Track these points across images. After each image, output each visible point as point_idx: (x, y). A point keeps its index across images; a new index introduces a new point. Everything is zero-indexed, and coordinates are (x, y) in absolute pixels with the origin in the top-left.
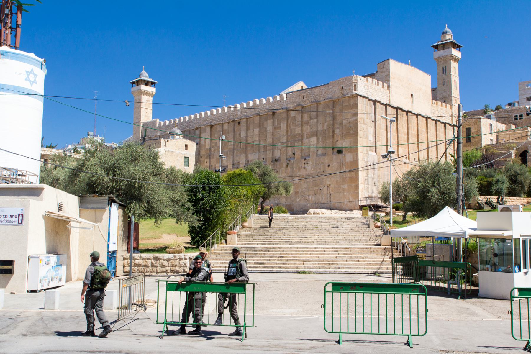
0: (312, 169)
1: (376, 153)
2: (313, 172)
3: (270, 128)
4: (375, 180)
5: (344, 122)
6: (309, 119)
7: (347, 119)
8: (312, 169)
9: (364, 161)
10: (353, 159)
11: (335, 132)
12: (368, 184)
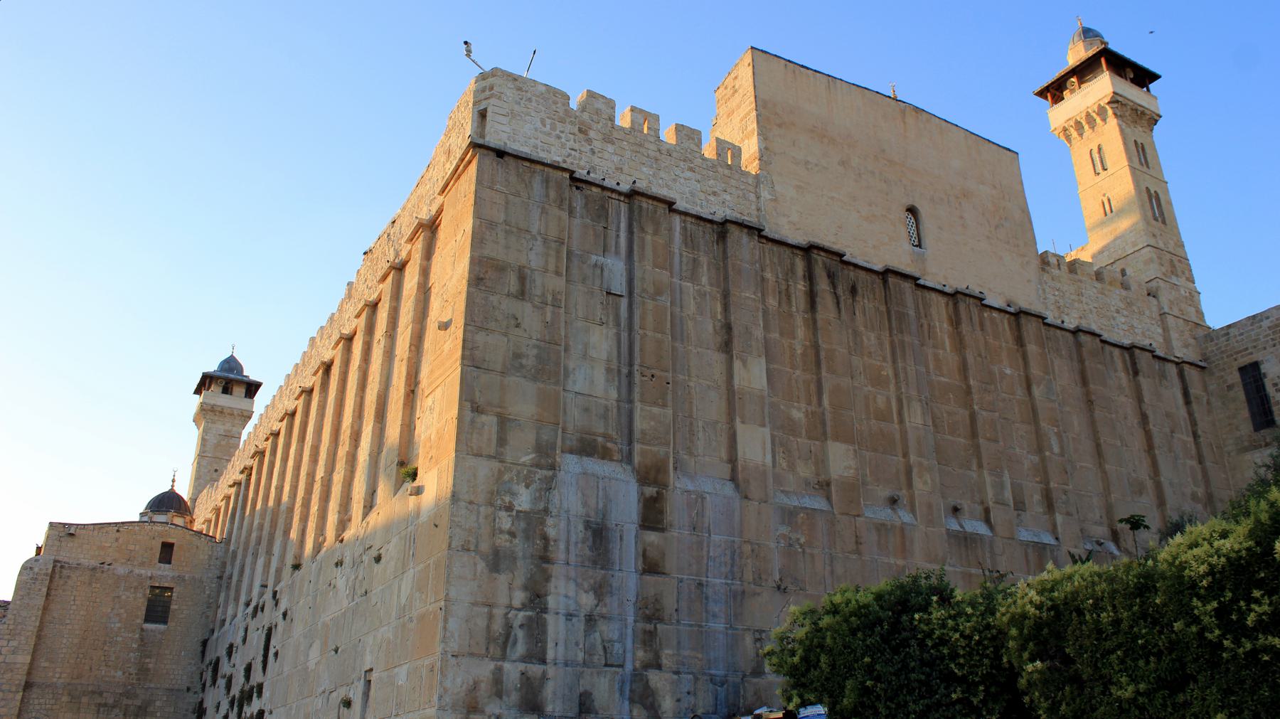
4: (608, 630)
9: (509, 508)
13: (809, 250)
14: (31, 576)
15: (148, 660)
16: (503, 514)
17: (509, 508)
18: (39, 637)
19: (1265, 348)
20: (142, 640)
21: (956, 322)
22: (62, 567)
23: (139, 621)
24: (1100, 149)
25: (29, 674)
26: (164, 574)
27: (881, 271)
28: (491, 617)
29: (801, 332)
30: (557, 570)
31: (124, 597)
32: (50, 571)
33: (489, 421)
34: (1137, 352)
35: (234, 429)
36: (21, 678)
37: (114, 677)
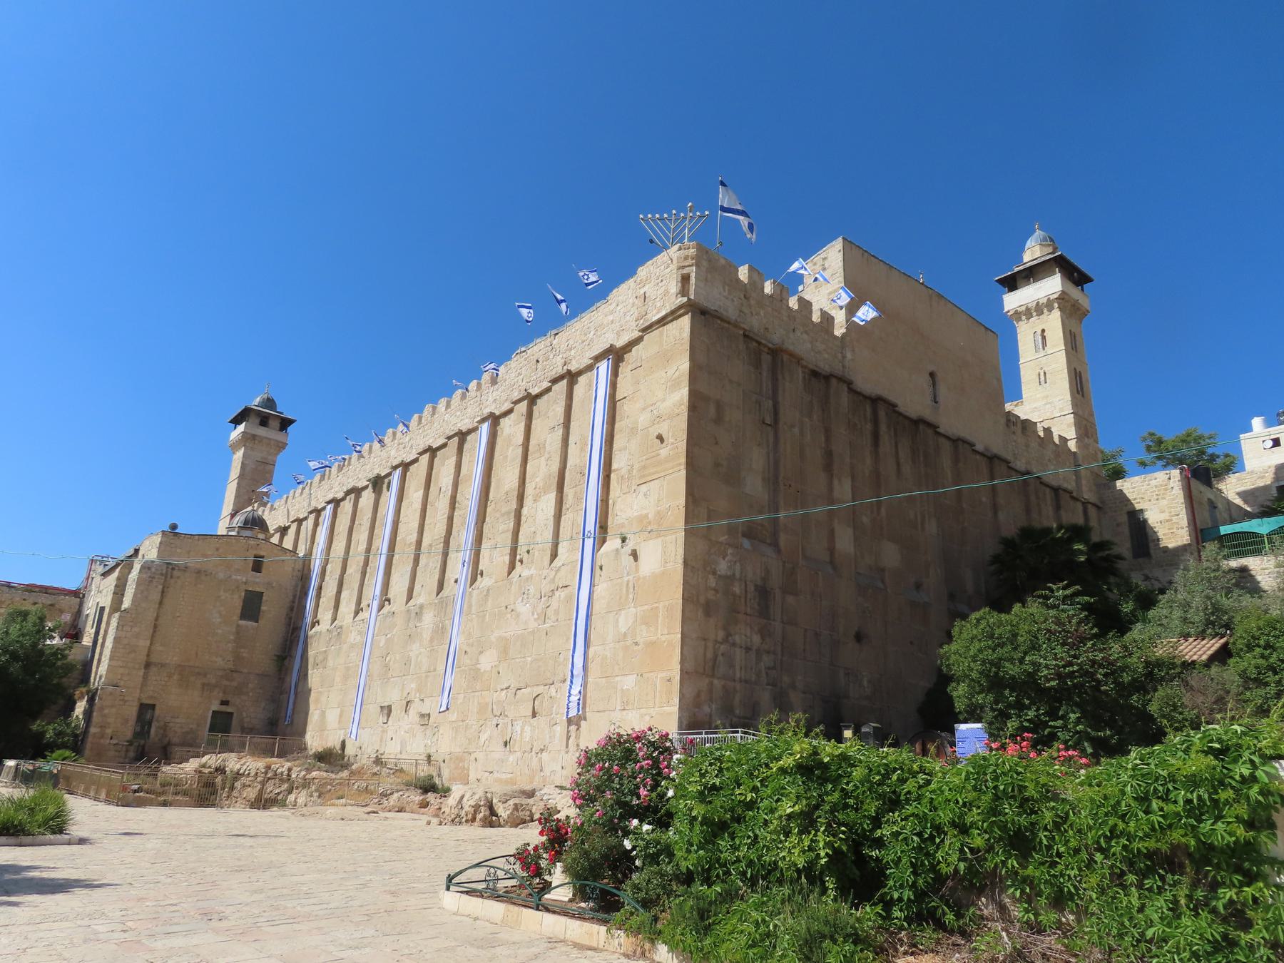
0: (533, 614)
8: (533, 614)
9: (714, 573)
13: (876, 401)
14: (149, 574)
15: (242, 650)
16: (711, 576)
17: (714, 573)
18: (155, 627)
19: (1150, 501)
20: (238, 633)
21: (956, 460)
22: (173, 569)
23: (235, 618)
24: (1043, 331)
25: (148, 655)
26: (257, 582)
27: (915, 418)
28: (706, 647)
29: (869, 461)
31: (223, 598)
32: (164, 572)
34: (1061, 492)
35: (270, 457)
36: (142, 658)
37: (216, 662)
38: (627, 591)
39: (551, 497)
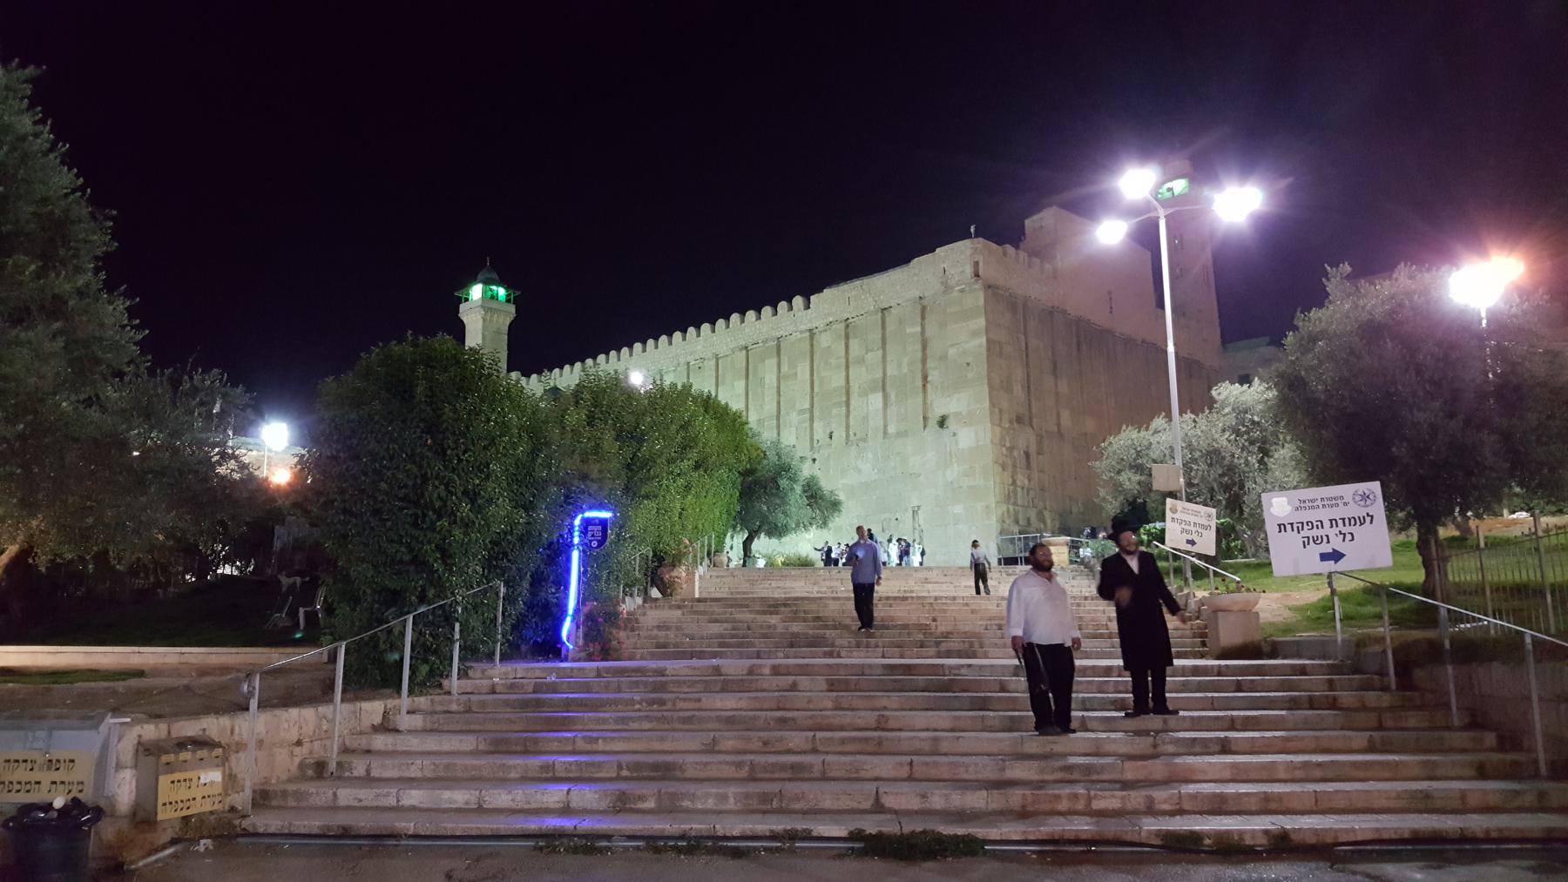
0: (873, 470)
1: (1033, 429)
2: (876, 477)
3: (770, 378)
4: (1032, 493)
5: (951, 352)
6: (864, 352)
7: (958, 344)
8: (873, 470)
10: (978, 441)
11: (929, 378)
12: (1015, 504)
16: (1004, 448)
30: (1019, 470)
33: (997, 410)
38: (951, 456)
39: (879, 396)
